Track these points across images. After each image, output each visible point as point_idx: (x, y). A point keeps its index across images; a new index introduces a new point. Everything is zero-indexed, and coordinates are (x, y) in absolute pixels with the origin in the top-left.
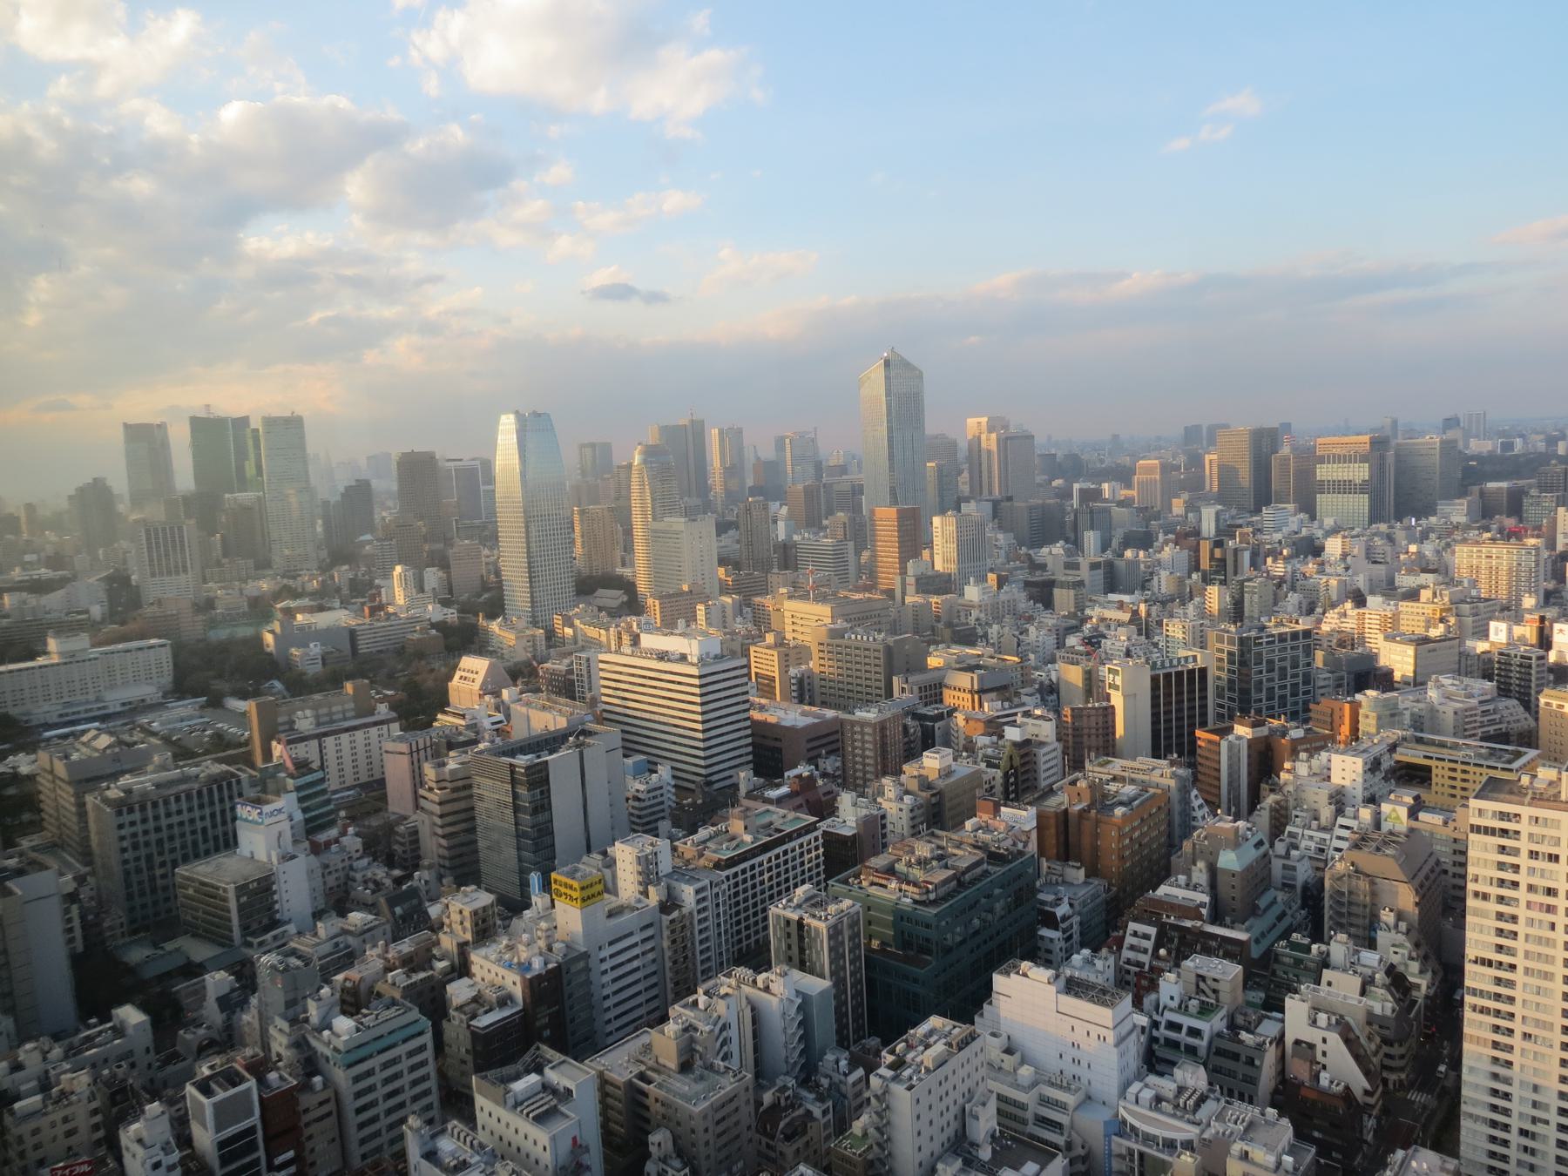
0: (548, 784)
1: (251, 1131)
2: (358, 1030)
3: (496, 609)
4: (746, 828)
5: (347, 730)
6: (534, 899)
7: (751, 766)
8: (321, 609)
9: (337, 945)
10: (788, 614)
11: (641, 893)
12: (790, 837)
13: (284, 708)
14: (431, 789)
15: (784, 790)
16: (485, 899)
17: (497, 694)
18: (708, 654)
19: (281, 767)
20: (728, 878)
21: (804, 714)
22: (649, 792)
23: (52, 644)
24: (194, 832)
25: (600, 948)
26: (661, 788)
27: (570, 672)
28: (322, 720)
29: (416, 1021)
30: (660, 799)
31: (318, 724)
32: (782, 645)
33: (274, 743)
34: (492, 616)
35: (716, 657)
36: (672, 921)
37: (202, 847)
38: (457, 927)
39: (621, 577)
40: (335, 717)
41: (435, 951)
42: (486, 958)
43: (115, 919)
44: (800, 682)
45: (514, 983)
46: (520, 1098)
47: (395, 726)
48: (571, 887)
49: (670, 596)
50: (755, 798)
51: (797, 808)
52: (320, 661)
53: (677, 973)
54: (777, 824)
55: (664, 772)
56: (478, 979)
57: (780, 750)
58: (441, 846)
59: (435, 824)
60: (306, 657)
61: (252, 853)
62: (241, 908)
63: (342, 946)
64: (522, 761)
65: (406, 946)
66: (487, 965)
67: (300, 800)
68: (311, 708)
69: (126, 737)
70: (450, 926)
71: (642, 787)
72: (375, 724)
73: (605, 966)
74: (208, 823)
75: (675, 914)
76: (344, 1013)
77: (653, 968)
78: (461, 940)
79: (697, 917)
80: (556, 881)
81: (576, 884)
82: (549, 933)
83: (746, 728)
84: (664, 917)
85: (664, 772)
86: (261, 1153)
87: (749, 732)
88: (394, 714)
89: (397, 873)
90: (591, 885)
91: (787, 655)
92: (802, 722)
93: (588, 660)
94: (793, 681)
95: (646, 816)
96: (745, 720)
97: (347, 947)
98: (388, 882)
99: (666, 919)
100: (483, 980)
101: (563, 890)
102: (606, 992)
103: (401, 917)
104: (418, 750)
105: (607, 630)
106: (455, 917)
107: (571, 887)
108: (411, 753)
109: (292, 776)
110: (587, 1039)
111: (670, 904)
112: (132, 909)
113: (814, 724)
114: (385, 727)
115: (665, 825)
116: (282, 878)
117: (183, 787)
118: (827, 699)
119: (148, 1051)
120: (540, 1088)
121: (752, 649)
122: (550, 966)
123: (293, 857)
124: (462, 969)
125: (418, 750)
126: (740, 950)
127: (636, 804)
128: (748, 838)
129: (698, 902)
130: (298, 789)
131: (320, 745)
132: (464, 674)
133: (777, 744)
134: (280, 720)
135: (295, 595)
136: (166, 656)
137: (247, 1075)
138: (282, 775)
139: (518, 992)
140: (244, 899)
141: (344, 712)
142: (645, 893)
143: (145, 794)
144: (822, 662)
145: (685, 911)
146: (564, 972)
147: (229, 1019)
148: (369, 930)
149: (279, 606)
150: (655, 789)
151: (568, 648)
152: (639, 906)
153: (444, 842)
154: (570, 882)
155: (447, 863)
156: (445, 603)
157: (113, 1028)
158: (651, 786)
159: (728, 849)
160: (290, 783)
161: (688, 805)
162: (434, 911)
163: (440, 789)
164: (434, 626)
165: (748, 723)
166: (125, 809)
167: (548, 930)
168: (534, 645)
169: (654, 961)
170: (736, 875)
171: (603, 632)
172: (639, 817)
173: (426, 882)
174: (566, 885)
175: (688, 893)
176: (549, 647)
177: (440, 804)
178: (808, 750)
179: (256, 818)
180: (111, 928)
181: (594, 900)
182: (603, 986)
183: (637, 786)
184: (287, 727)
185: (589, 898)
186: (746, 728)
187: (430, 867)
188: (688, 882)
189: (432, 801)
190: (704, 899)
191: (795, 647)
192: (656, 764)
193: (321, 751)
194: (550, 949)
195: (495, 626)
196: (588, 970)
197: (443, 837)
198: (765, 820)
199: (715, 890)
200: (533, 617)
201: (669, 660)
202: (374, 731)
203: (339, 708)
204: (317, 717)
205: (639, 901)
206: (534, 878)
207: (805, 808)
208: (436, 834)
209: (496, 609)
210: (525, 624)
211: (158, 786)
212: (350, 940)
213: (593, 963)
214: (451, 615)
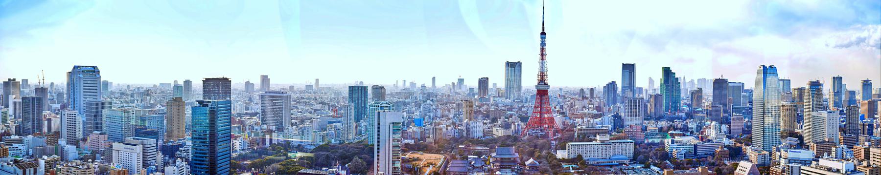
52: (683, 155)
132: (741, 168)
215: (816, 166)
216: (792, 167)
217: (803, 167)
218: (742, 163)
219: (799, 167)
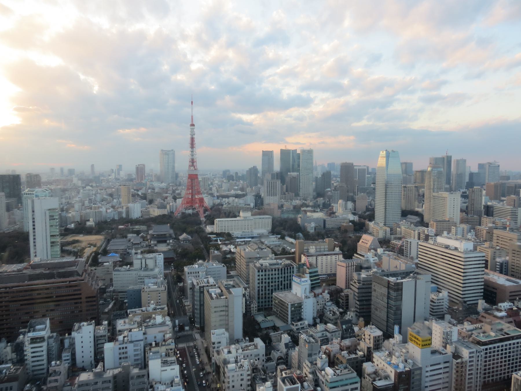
0: (402, 291)
2: (334, 375)
3: (372, 218)
4: (492, 329)
5: (325, 255)
6: (395, 336)
7: (482, 297)
8: (314, 211)
9: (323, 334)
10: (494, 235)
11: (443, 346)
12: (513, 338)
13: (306, 245)
14: (355, 282)
15: (503, 314)
16: (379, 333)
17: (376, 251)
18: (467, 249)
19: (304, 264)
20: (483, 349)
21: (508, 280)
22: (438, 300)
23: (241, 214)
24: (278, 282)
25: (427, 367)
26: (443, 299)
27: (402, 246)
28: (317, 250)
29: (355, 378)
30: (442, 304)
31: (316, 251)
32: (492, 248)
33: (302, 256)
34: (370, 220)
35: (471, 251)
36: (457, 363)
37: (280, 287)
38: (367, 341)
39: (417, 212)
40: (321, 250)
41: (358, 347)
42: (380, 357)
43: (254, 306)
44: (501, 264)
45: (391, 372)
47: (341, 256)
48: (417, 339)
49: (440, 221)
50: (489, 314)
51: (510, 322)
53: (457, 385)
54: (506, 330)
55: (444, 294)
56: (375, 364)
57: (495, 293)
58: (356, 303)
59: (355, 295)
60: (311, 227)
61: (296, 293)
62: (292, 312)
63: (324, 335)
64: (392, 279)
65: (347, 342)
66: (380, 360)
67: (311, 277)
68: (316, 246)
69: (260, 246)
70: (364, 339)
71: (435, 297)
72: (335, 254)
73: (428, 374)
74: (283, 279)
75: (459, 361)
76: (329, 366)
77: (447, 380)
78: (368, 346)
79: (469, 364)
80: (411, 335)
81: (420, 338)
82: (406, 355)
83: (481, 282)
84: (454, 360)
85: (444, 294)
87: (483, 283)
88: (341, 252)
89: (341, 310)
91: (495, 252)
92: (508, 284)
93: (411, 242)
94: (498, 264)
95: (436, 309)
96: (482, 278)
97: (326, 336)
98: (338, 313)
99: (455, 361)
100: (378, 365)
101: (413, 339)
102: (427, 385)
103: (345, 329)
104: (349, 266)
105: (414, 231)
106: (367, 337)
107: (417, 339)
108: (347, 267)
109: (308, 268)
111: (456, 356)
112: (259, 302)
113: (514, 286)
114: (338, 256)
115: (448, 317)
117: (277, 266)
118: (515, 274)
119: (263, 355)
121: (478, 247)
122: (407, 369)
123: (309, 298)
124: (369, 358)
125: (349, 266)
126: (484, 382)
127: (432, 304)
128: (493, 334)
129: (470, 357)
130: (310, 273)
131: (316, 259)
132: (363, 241)
133: (495, 291)
134: (305, 248)
135: (307, 206)
136: (270, 221)
137: (298, 382)
138: (305, 267)
140: (293, 309)
141: (324, 249)
142: (445, 347)
143: (266, 266)
144: (513, 258)
145: (464, 360)
146: (412, 373)
147: (288, 351)
148: (334, 332)
150: (441, 299)
151: (398, 236)
152: (444, 352)
153: (358, 303)
154: (417, 337)
155: (358, 310)
156: (354, 214)
157: (254, 345)
158: (439, 298)
159: (483, 337)
160: (308, 271)
161: (456, 309)
162: (356, 329)
163: (358, 283)
164: (351, 221)
165: (483, 280)
166: (260, 270)
167: (405, 353)
168: (386, 233)
169: (448, 377)
170: (486, 349)
171: (412, 232)
172: (433, 309)
173: (352, 317)
174: (415, 338)
175: (465, 353)
176: (391, 234)
177: (358, 289)
178: (510, 296)
179: (299, 282)
180: (253, 308)
181: (426, 346)
182: (426, 382)
183: (433, 296)
184: (307, 251)
185: (425, 345)
186: (481, 282)
187: (354, 312)
188: (465, 347)
189: (355, 287)
190: (473, 357)
191: (499, 249)
192: (441, 289)
193: (316, 261)
194: (406, 361)
195: (371, 224)
196: (420, 374)
197: (358, 301)
198: (500, 327)
199: (478, 354)
200: (385, 223)
201: (450, 249)
202: (334, 257)
203: (323, 247)
204: (316, 249)
205: (443, 350)
206: (396, 328)
207: (514, 324)
208: (355, 299)
209: (372, 218)
210: (383, 225)
211: (270, 265)
212: (328, 334)
213: (423, 372)
214: (356, 218)
215: (434, 243)
217: (420, 243)
218: (365, 237)
219: (418, 243)
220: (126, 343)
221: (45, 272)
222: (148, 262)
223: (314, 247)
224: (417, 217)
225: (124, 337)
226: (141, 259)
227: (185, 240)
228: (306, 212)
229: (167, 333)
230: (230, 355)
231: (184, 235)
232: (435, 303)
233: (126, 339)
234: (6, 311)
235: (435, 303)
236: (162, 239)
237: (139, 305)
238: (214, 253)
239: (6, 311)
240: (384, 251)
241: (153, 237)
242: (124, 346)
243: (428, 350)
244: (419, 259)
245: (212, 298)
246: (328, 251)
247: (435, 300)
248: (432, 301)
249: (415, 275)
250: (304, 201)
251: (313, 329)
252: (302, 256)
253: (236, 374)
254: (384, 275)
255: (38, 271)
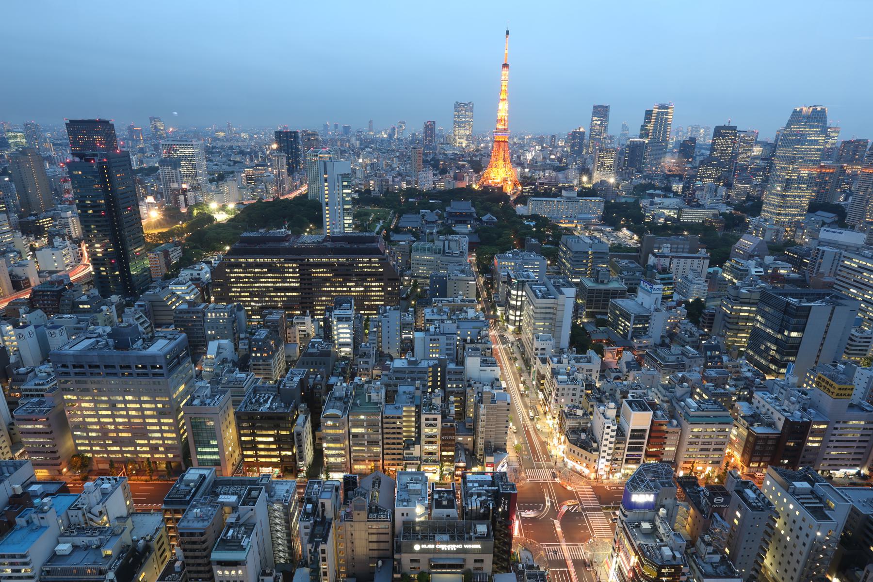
1: (644, 431)
8: (665, 196)
17: (763, 259)
19: (654, 267)
22: (861, 338)
46: (797, 491)
71: (856, 334)
81: (835, 384)
86: (646, 441)
90: (846, 389)
98: (697, 334)
110: (810, 462)
116: (653, 318)
120: (809, 491)
123: (660, 311)
127: (850, 342)
135: (655, 188)
139: (780, 425)
141: (683, 249)
148: (695, 357)
149: (648, 192)
156: (728, 204)
157: (586, 357)
160: (658, 276)
185: (841, 395)
194: (805, 410)
203: (682, 246)
204: (671, 248)
214: (728, 210)
216: (824, 251)
220: (438, 335)
221: (345, 247)
222: (453, 245)
223: (669, 245)
224: (834, 215)
225: (435, 328)
226: (444, 241)
227: (490, 222)
228: (652, 196)
229: (483, 330)
230: (560, 365)
231: (489, 215)
232: (855, 341)
233: (437, 330)
234: (308, 284)
235: (855, 341)
236: (462, 219)
237: (443, 294)
238: (531, 241)
239: (308, 284)
240: (775, 260)
241: (450, 214)
242: (436, 337)
243: (846, 402)
244: (838, 277)
245: (537, 296)
246: (689, 253)
247: (856, 337)
248: (851, 339)
249: (833, 299)
250: (650, 181)
251: (665, 350)
252: (650, 255)
253: (566, 387)
254: (780, 294)
255: (338, 245)
